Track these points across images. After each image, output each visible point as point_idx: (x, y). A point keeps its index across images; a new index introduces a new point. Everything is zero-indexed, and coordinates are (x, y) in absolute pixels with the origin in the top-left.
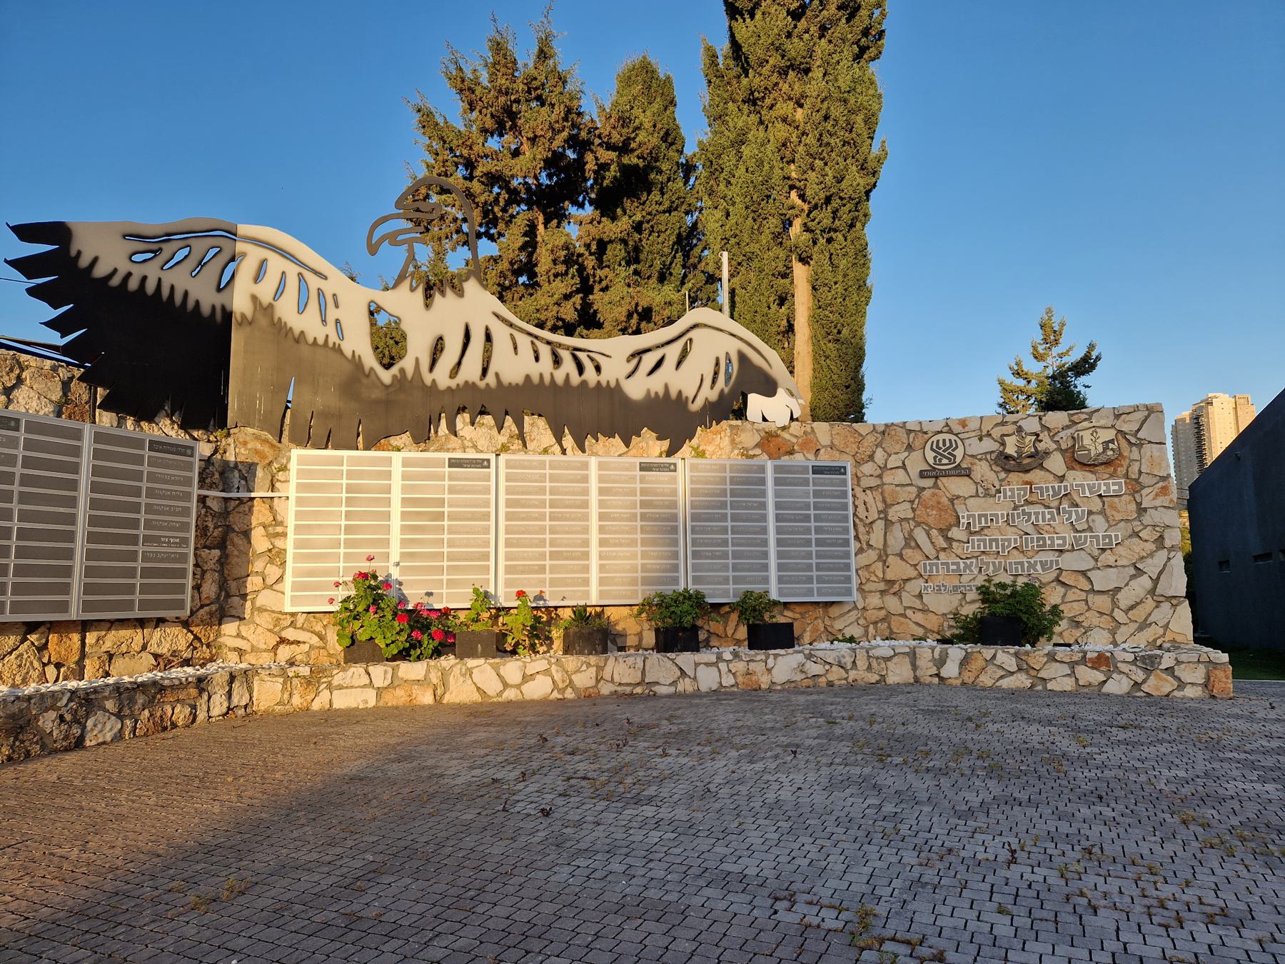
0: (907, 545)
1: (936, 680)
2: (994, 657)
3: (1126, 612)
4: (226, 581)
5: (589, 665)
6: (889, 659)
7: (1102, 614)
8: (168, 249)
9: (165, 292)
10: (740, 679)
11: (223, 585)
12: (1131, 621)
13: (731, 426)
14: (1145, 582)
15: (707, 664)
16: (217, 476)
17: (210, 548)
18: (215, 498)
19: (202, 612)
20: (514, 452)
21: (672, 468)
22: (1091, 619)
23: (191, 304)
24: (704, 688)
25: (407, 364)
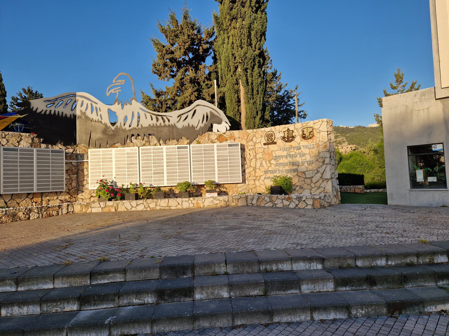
0: (261, 166)
1: (251, 205)
2: (264, 198)
3: (314, 184)
5: (153, 202)
6: (239, 199)
7: (308, 185)
8: (56, 103)
9: (57, 113)
10: (195, 205)
11: (78, 183)
12: (316, 186)
14: (319, 175)
15: (185, 201)
20: (147, 146)
21: (186, 148)
22: (305, 186)
23: (64, 115)
24: (184, 207)
25: (118, 124)
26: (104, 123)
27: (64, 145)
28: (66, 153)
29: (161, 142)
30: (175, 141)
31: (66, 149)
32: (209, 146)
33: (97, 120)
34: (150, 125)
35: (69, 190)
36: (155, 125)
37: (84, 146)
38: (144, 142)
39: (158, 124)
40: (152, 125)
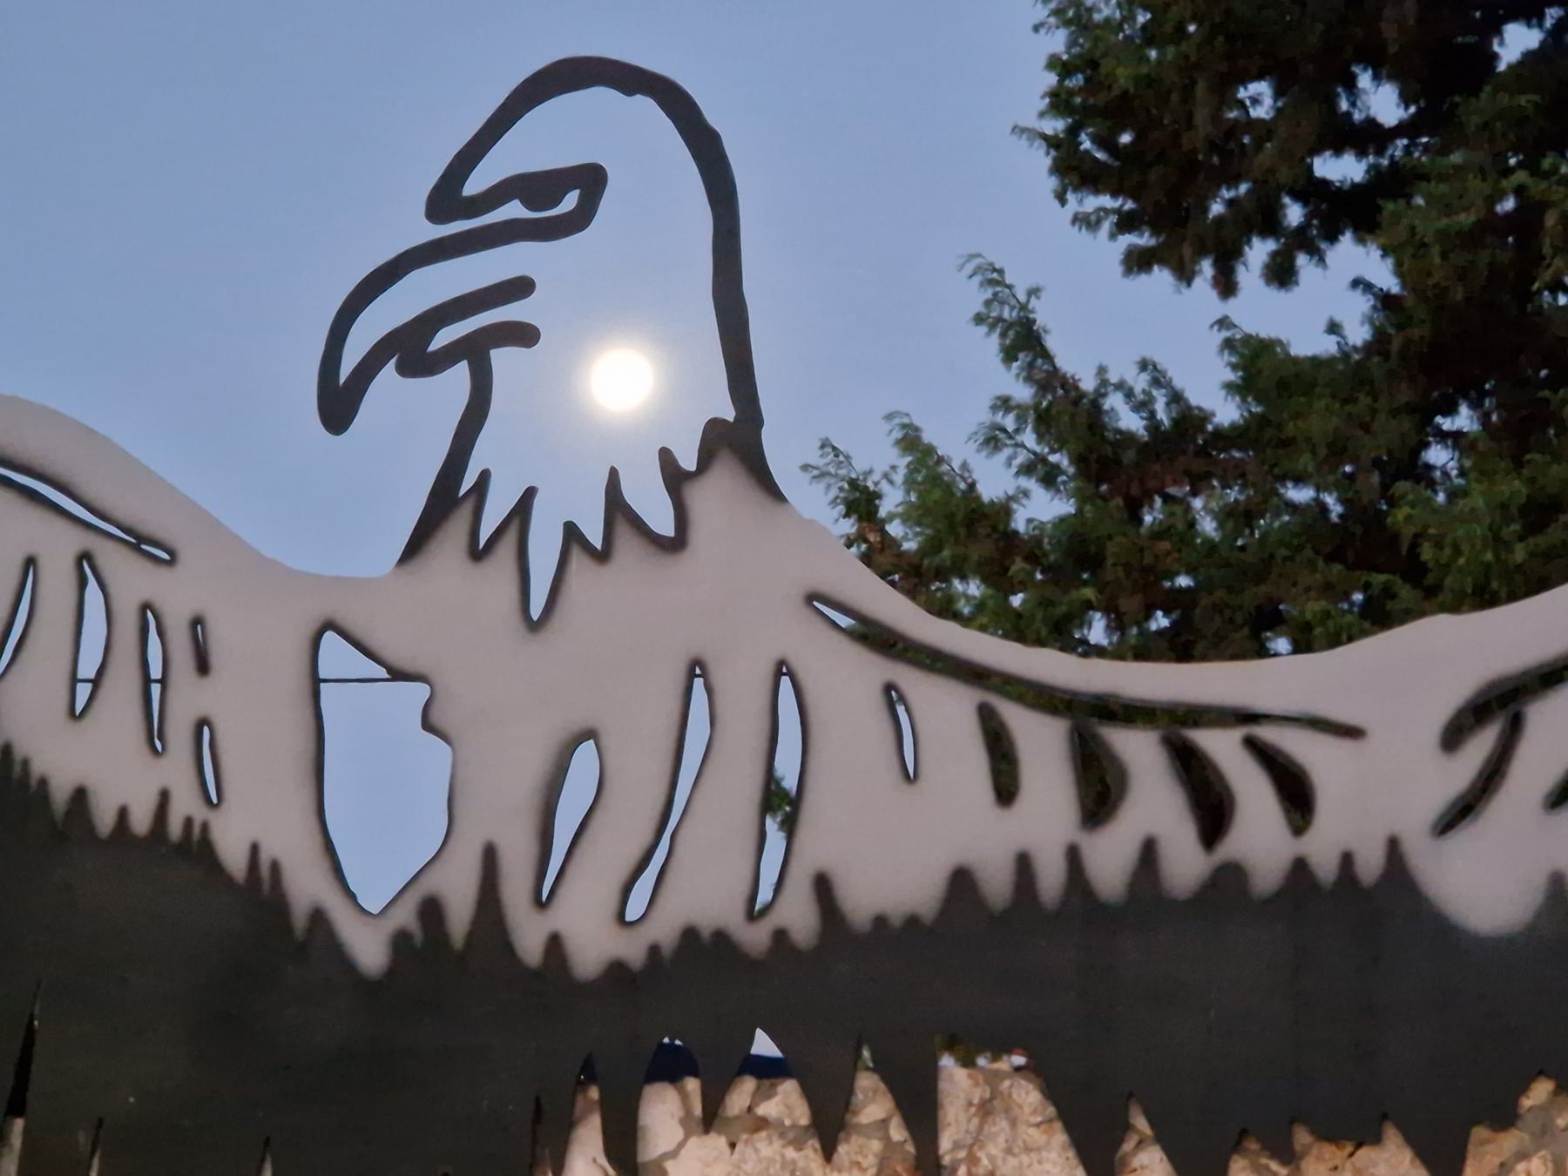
33: (141, 822)
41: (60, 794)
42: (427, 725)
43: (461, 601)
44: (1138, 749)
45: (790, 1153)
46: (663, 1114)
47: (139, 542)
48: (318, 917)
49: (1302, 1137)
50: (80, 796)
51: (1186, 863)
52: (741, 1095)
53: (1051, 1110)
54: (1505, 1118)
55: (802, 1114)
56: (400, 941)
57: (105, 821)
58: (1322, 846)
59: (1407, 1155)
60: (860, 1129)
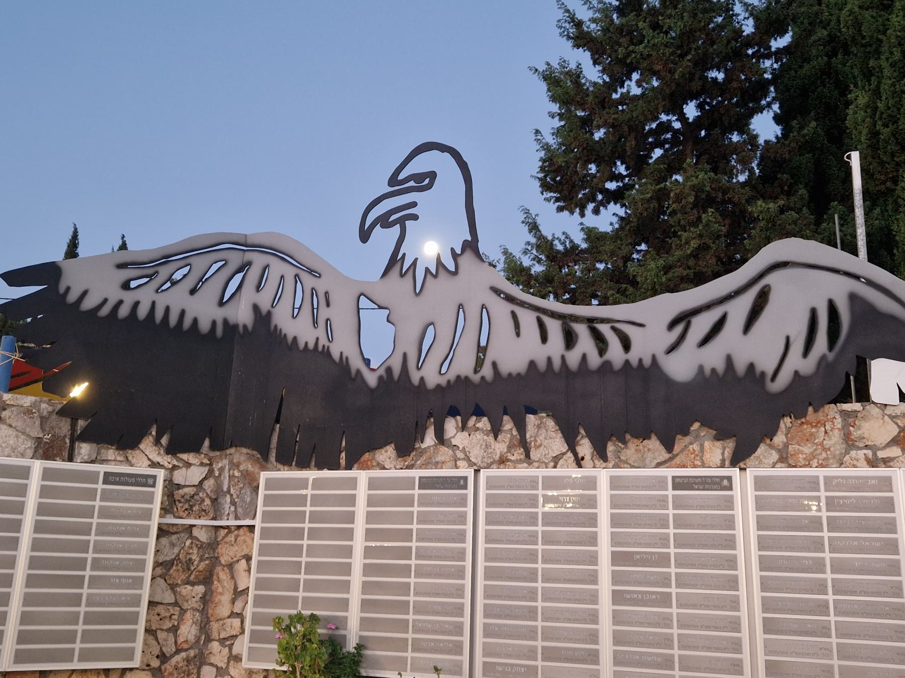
4: (208, 621)
8: (164, 272)
9: (159, 315)
13: (845, 414)
16: (207, 502)
17: (193, 584)
18: (203, 526)
19: (178, 658)
26: (336, 356)
27: (172, 450)
28: (171, 487)
29: (585, 448)
30: (654, 443)
31: (175, 468)
32: (861, 484)
33: (311, 346)
34: (532, 364)
35: (163, 657)
36: (557, 363)
37: (250, 457)
38: (500, 447)
39: (573, 358)
40: (542, 365)
41: (290, 339)
42: (388, 321)
43: (398, 287)
44: (581, 330)
45: (485, 437)
46: (451, 426)
47: (311, 271)
48: (358, 372)
49: (628, 436)
50: (295, 338)
51: (595, 360)
52: (472, 421)
53: (557, 428)
54: (686, 433)
55: (489, 427)
56: (380, 378)
57: (301, 345)
58: (634, 356)
59: (658, 442)
60: (505, 431)
